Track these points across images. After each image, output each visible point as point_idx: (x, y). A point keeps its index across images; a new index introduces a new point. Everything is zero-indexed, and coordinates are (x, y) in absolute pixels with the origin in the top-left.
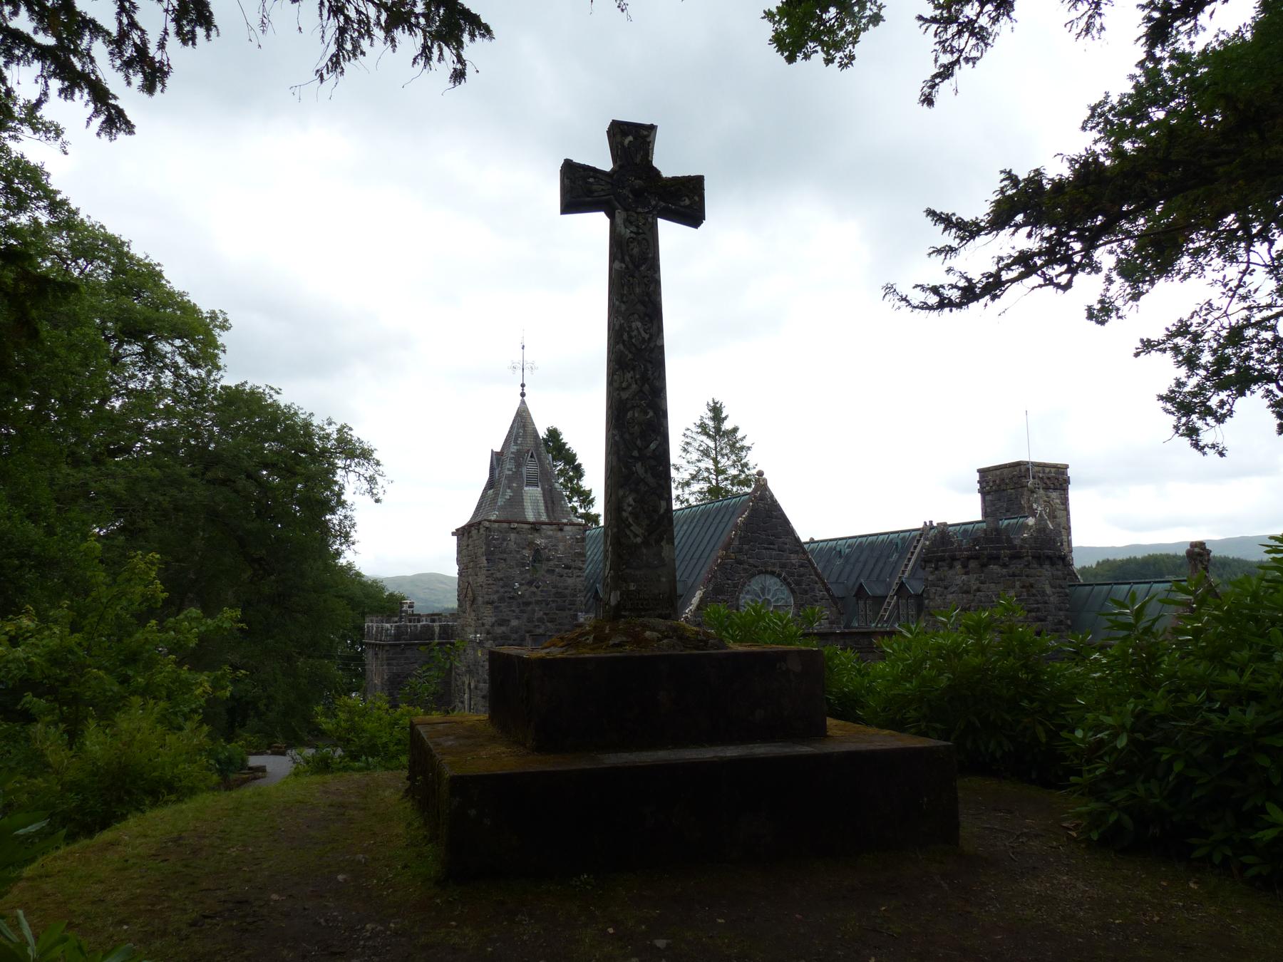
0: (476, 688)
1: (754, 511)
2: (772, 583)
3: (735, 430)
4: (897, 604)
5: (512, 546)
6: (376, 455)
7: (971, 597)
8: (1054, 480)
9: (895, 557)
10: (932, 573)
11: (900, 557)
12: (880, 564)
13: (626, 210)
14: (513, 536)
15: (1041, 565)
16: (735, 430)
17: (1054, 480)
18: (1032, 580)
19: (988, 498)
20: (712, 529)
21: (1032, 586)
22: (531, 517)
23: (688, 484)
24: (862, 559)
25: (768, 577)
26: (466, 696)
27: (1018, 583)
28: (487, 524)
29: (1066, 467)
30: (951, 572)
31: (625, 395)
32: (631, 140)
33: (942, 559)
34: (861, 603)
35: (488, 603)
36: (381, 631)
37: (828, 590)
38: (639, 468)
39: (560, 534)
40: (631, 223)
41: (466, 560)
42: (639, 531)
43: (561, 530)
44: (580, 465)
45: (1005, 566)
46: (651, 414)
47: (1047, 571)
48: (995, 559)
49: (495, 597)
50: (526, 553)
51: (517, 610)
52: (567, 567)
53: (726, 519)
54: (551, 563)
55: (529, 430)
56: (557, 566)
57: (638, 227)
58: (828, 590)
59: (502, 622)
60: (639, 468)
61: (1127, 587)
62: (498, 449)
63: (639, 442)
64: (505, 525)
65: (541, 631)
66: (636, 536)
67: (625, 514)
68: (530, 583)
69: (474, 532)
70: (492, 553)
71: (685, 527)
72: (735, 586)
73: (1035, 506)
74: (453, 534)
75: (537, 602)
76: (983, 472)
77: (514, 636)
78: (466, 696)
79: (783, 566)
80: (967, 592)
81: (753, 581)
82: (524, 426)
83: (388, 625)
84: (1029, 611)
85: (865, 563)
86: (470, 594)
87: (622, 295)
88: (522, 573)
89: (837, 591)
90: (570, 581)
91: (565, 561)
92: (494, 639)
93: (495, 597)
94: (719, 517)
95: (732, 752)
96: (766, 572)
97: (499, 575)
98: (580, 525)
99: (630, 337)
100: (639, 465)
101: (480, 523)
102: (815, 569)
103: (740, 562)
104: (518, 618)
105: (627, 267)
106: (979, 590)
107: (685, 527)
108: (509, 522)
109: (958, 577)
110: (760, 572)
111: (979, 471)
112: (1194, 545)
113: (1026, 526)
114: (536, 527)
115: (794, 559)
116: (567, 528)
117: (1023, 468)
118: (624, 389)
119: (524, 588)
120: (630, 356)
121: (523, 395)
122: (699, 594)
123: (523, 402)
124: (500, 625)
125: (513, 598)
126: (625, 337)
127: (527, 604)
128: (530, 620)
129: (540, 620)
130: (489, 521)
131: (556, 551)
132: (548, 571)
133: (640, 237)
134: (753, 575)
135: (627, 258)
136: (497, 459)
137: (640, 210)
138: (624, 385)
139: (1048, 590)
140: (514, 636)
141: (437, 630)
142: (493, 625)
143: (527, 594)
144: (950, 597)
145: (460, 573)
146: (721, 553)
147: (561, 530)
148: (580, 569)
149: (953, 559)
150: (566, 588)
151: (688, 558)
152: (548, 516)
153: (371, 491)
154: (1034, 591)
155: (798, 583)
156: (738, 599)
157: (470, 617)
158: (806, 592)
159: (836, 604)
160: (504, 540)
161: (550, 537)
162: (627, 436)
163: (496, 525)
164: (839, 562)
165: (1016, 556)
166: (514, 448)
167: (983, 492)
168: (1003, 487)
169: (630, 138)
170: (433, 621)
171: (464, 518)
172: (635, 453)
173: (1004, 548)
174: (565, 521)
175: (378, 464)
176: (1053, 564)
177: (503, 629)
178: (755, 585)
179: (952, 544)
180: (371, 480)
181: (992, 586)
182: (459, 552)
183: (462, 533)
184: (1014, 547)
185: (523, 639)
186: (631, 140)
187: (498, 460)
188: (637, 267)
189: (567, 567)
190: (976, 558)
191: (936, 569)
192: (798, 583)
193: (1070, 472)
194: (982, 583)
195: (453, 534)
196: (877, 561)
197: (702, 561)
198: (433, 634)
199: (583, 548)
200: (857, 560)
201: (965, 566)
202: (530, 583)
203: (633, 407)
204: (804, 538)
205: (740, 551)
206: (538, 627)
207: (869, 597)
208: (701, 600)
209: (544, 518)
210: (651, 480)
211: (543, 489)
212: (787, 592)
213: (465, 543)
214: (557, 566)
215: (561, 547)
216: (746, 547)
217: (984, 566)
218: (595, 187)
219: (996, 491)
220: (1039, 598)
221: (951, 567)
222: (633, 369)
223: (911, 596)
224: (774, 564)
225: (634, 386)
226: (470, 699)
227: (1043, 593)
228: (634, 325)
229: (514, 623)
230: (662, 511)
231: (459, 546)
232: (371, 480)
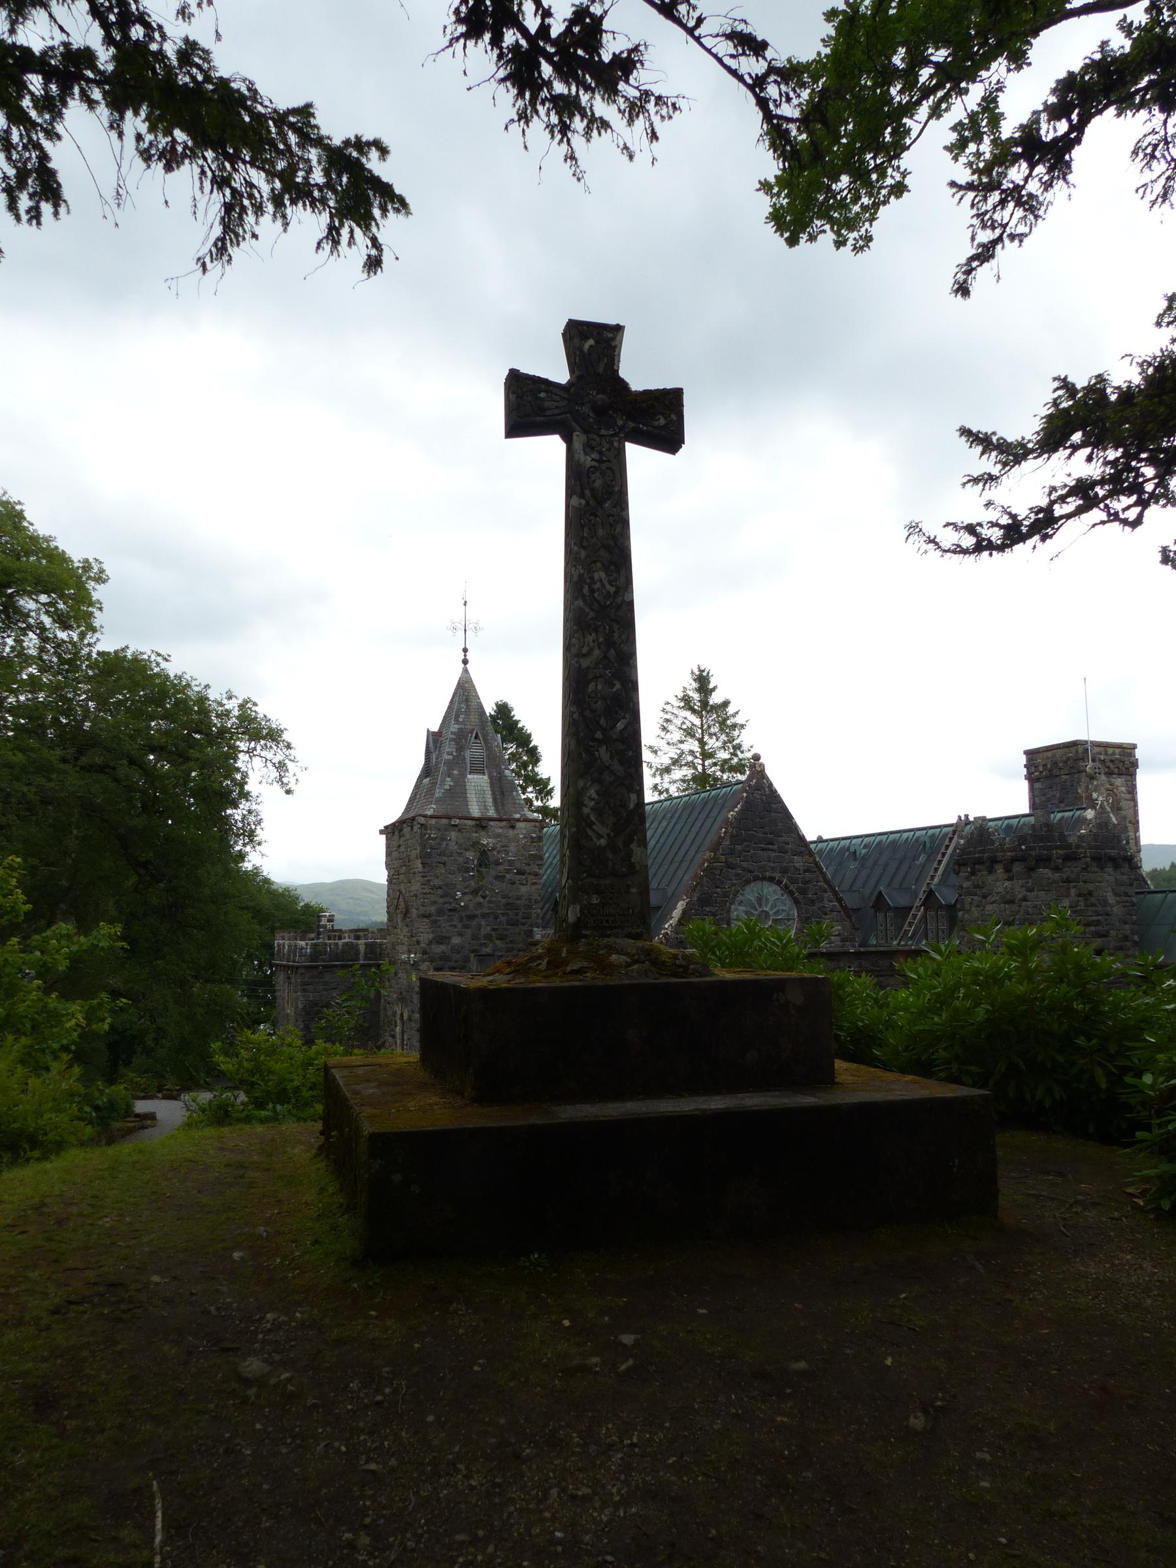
0: (410, 1019)
1: (749, 805)
2: (771, 892)
3: (726, 704)
4: (924, 917)
5: (453, 846)
6: (286, 736)
7: (1015, 907)
8: (1119, 762)
10: (967, 879)
11: (928, 859)
13: (586, 432)
14: (453, 835)
15: (1102, 868)
16: (726, 704)
17: (1119, 762)
18: (1090, 887)
19: (1037, 785)
20: (698, 824)
21: (1090, 894)
22: (475, 811)
23: (667, 770)
25: (766, 883)
26: (398, 1029)
27: (1073, 891)
28: (422, 820)
29: (1134, 747)
30: (991, 878)
31: (585, 663)
32: (593, 343)
33: (980, 862)
34: (880, 916)
35: (424, 916)
36: (294, 950)
37: (840, 900)
38: (603, 753)
39: (511, 832)
40: (592, 448)
41: (396, 864)
42: (604, 831)
43: (513, 827)
44: (535, 748)
45: (1056, 869)
46: (618, 686)
47: (1109, 875)
48: (1044, 861)
49: (433, 909)
50: (470, 855)
51: (459, 925)
52: (520, 872)
53: (714, 814)
54: (501, 868)
55: (473, 704)
56: (508, 871)
57: (600, 453)
58: (840, 900)
59: (441, 940)
60: (603, 753)
62: (435, 728)
63: (603, 721)
64: (444, 821)
65: (488, 950)
66: (600, 836)
67: (586, 810)
68: (475, 892)
69: (406, 830)
70: (429, 855)
71: (664, 824)
72: (726, 895)
73: (1095, 795)
74: (381, 832)
75: (484, 916)
76: (1031, 754)
78: (398, 1029)
79: (784, 871)
80: (1011, 902)
81: (748, 889)
82: (467, 700)
83: (303, 943)
84: (1087, 925)
85: (886, 865)
86: (402, 905)
87: (582, 539)
88: (464, 879)
89: (851, 901)
91: (518, 865)
92: (432, 960)
93: (433, 909)
94: (707, 810)
95: (717, 1103)
96: (764, 879)
97: (437, 882)
98: (535, 821)
99: (592, 591)
100: (603, 750)
101: (413, 819)
103: (732, 866)
104: (461, 935)
105: (587, 504)
106: (1025, 899)
107: (664, 824)
108: (450, 818)
109: (999, 882)
110: (756, 879)
111: (1026, 752)
113: (1083, 821)
114: (482, 824)
115: (798, 862)
117: (1080, 749)
118: (584, 656)
119: (467, 898)
120: (592, 614)
121: (465, 662)
122: (681, 905)
123: (466, 671)
124: (438, 943)
125: (453, 910)
126: (586, 590)
127: (472, 917)
128: (475, 937)
129: (488, 937)
130: (425, 816)
132: (497, 877)
133: (603, 466)
134: (748, 882)
135: (587, 492)
136: (434, 741)
137: (603, 432)
138: (585, 650)
139: (1111, 899)
141: (362, 949)
142: (430, 943)
143: (471, 906)
144: (989, 907)
145: (390, 880)
146: (709, 855)
147: (513, 827)
148: (536, 875)
149: (994, 860)
150: (519, 898)
152: (497, 810)
153: (280, 780)
154: (1093, 900)
155: (803, 892)
156: (729, 911)
157: (403, 933)
158: (812, 902)
159: (849, 917)
160: (443, 839)
161: (499, 835)
162: (588, 713)
163: (433, 821)
164: (853, 866)
165: (1071, 857)
166: (454, 728)
167: (1030, 778)
168: (1055, 772)
169: (591, 342)
170: (358, 938)
171: (394, 811)
172: (599, 735)
173: (1056, 848)
174: (517, 816)
175: (289, 746)
176: (1117, 867)
177: (443, 947)
178: (750, 893)
179: (993, 842)
180: (281, 766)
182: (388, 854)
183: (392, 832)
184: (1069, 846)
185: (467, 960)
186: (593, 343)
187: (435, 742)
188: (600, 503)
189: (520, 872)
190: (1022, 859)
191: (973, 873)
192: (803, 892)
193: (1138, 753)
194: (1030, 890)
195: (381, 832)
196: (901, 863)
197: (685, 865)
198: (357, 953)
199: (540, 849)
200: (875, 863)
201: (1008, 870)
202: (475, 892)
203: (596, 678)
204: (810, 836)
205: (732, 852)
206: (485, 945)
207: (890, 908)
208: (684, 912)
209: (492, 813)
210: (618, 768)
211: (491, 777)
213: (395, 844)
214: (508, 871)
215: (512, 848)
216: (739, 847)
217: (1032, 869)
218: (547, 404)
219: (1047, 777)
220: (1099, 908)
221: (991, 871)
222: (596, 630)
223: (941, 907)
224: (773, 869)
225: (597, 652)
226: (403, 1032)
227: (1105, 903)
228: (596, 576)
229: (456, 940)
230: (632, 806)
231: (388, 847)
232: (281, 766)
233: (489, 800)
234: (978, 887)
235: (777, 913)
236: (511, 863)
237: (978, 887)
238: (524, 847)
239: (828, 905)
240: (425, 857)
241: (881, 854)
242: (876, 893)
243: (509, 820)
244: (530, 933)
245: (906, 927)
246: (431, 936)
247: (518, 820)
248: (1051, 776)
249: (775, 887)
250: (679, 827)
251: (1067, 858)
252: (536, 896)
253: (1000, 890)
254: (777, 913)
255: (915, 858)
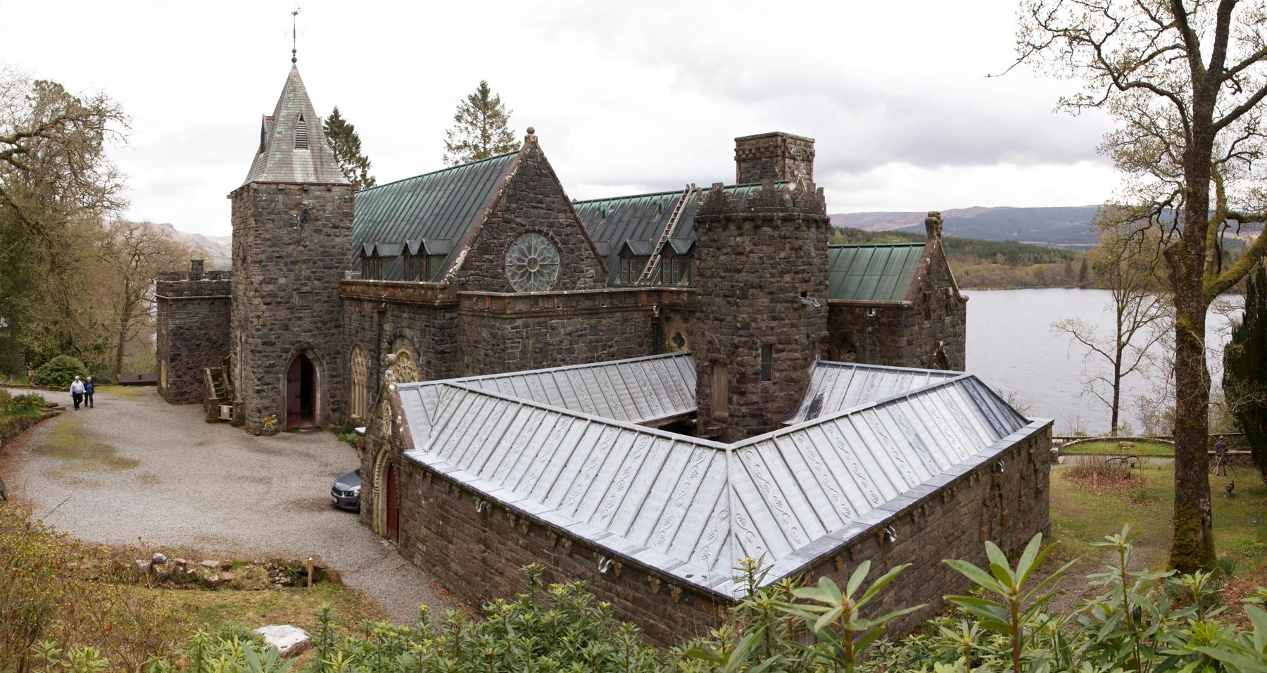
1: (523, 170)
7: (744, 258)
9: (658, 217)
10: (705, 234)
12: (644, 224)
14: (280, 197)
19: (743, 165)
20: (480, 187)
24: (625, 219)
30: (727, 233)
33: (717, 221)
34: (625, 262)
39: (328, 195)
43: (329, 190)
45: (776, 228)
47: (813, 233)
48: (768, 221)
49: (263, 257)
50: (294, 213)
51: (285, 269)
52: (335, 227)
53: (493, 177)
54: (320, 223)
56: (325, 226)
58: (593, 249)
61: (872, 250)
64: (274, 186)
68: (298, 243)
69: (245, 194)
70: (261, 214)
71: (452, 186)
74: (229, 197)
75: (304, 262)
76: (740, 141)
77: (283, 294)
79: (551, 226)
81: (520, 240)
84: (796, 273)
86: (241, 254)
88: (289, 233)
89: (602, 249)
90: (338, 240)
92: (262, 297)
93: (263, 257)
96: (534, 231)
97: (267, 236)
102: (582, 228)
103: (507, 221)
107: (452, 186)
108: (277, 184)
110: (528, 231)
112: (930, 215)
113: (788, 191)
114: (304, 188)
116: (334, 189)
122: (463, 254)
127: (295, 263)
129: (308, 278)
131: (324, 211)
132: (315, 231)
134: (521, 234)
139: (813, 253)
140: (283, 294)
142: (261, 283)
144: (722, 258)
145: (235, 235)
147: (329, 190)
149: (729, 220)
151: (454, 216)
156: (504, 258)
157: (241, 275)
158: (572, 251)
159: (601, 263)
161: (318, 197)
173: (777, 210)
177: (271, 287)
178: (522, 244)
181: (765, 248)
182: (233, 214)
183: (236, 196)
184: (786, 210)
185: (291, 297)
189: (335, 227)
194: (755, 244)
195: (229, 197)
199: (352, 207)
200: (620, 220)
201: (739, 228)
205: (508, 209)
206: (306, 285)
207: (633, 256)
209: (312, 179)
212: (553, 251)
214: (325, 226)
215: (329, 207)
216: (514, 206)
217: (757, 227)
221: (725, 229)
227: (809, 256)
229: (282, 281)
231: (233, 208)
233: (311, 169)
234: (714, 241)
235: (544, 259)
236: (328, 219)
237: (714, 241)
238: (339, 207)
239: (585, 254)
240: (257, 217)
241: (624, 213)
242: (621, 244)
243: (326, 185)
244: (343, 275)
245: (645, 271)
246: (261, 278)
247: (334, 185)
248: (755, 158)
249: (542, 238)
250: (464, 188)
251: (785, 220)
252: (347, 246)
253: (733, 243)
254: (544, 259)
255: (652, 217)
